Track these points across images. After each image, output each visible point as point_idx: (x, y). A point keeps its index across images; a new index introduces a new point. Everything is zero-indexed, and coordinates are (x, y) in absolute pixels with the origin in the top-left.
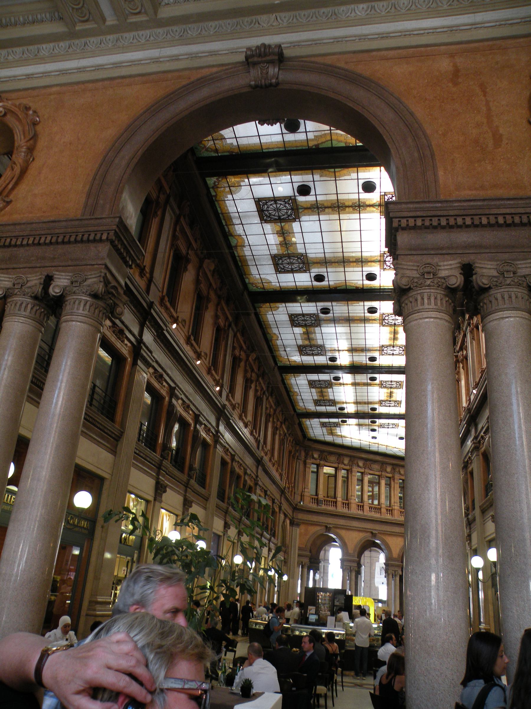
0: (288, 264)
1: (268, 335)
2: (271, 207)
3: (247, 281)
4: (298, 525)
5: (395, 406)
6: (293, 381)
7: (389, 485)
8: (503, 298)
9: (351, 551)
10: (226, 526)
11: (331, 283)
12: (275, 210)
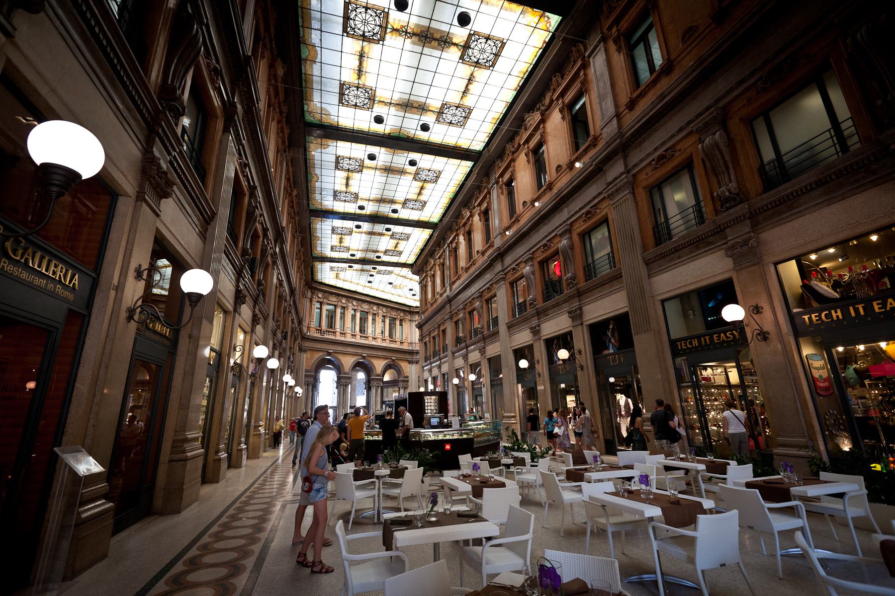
2: (360, 16)
3: (306, 107)
4: (305, 351)
6: (318, 226)
7: (374, 320)
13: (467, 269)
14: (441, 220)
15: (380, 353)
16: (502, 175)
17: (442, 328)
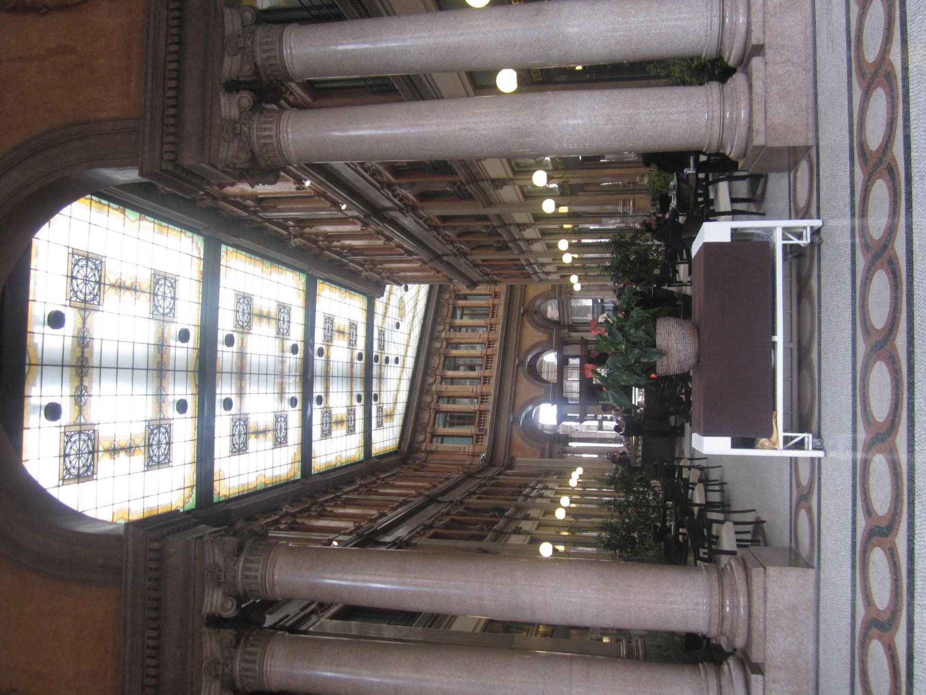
0: (159, 448)
1: (258, 488)
2: (73, 463)
5: (356, 329)
7: (457, 346)
8: (268, 51)
9: (542, 392)
10: (518, 531)
11: (189, 392)
12: (79, 458)
13: (389, 239)
14: (301, 271)
15: (513, 335)
16: (245, 208)
17: (480, 263)
